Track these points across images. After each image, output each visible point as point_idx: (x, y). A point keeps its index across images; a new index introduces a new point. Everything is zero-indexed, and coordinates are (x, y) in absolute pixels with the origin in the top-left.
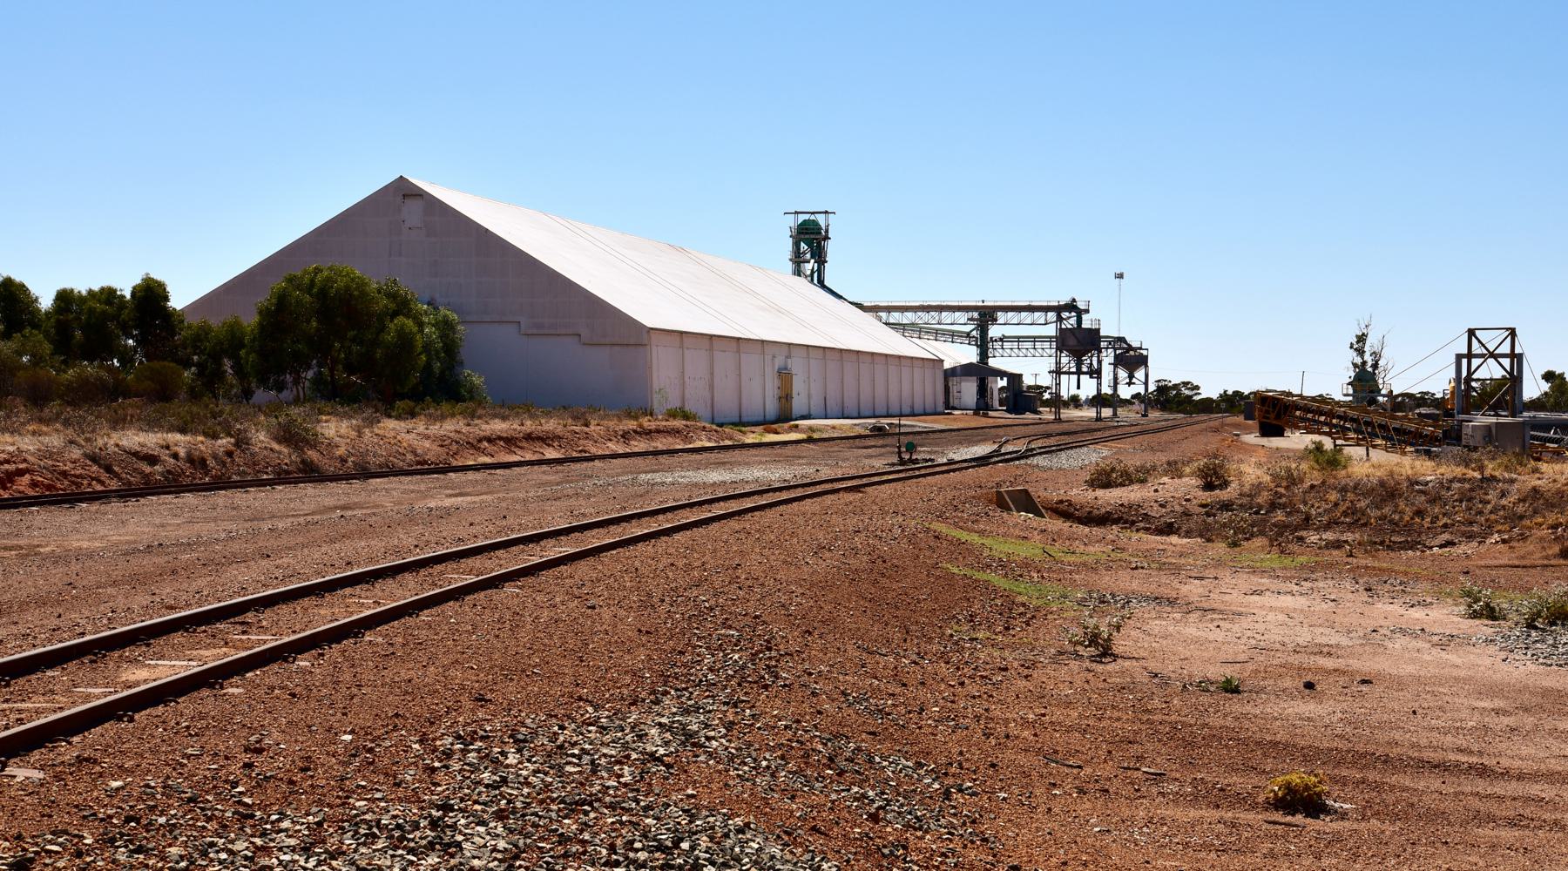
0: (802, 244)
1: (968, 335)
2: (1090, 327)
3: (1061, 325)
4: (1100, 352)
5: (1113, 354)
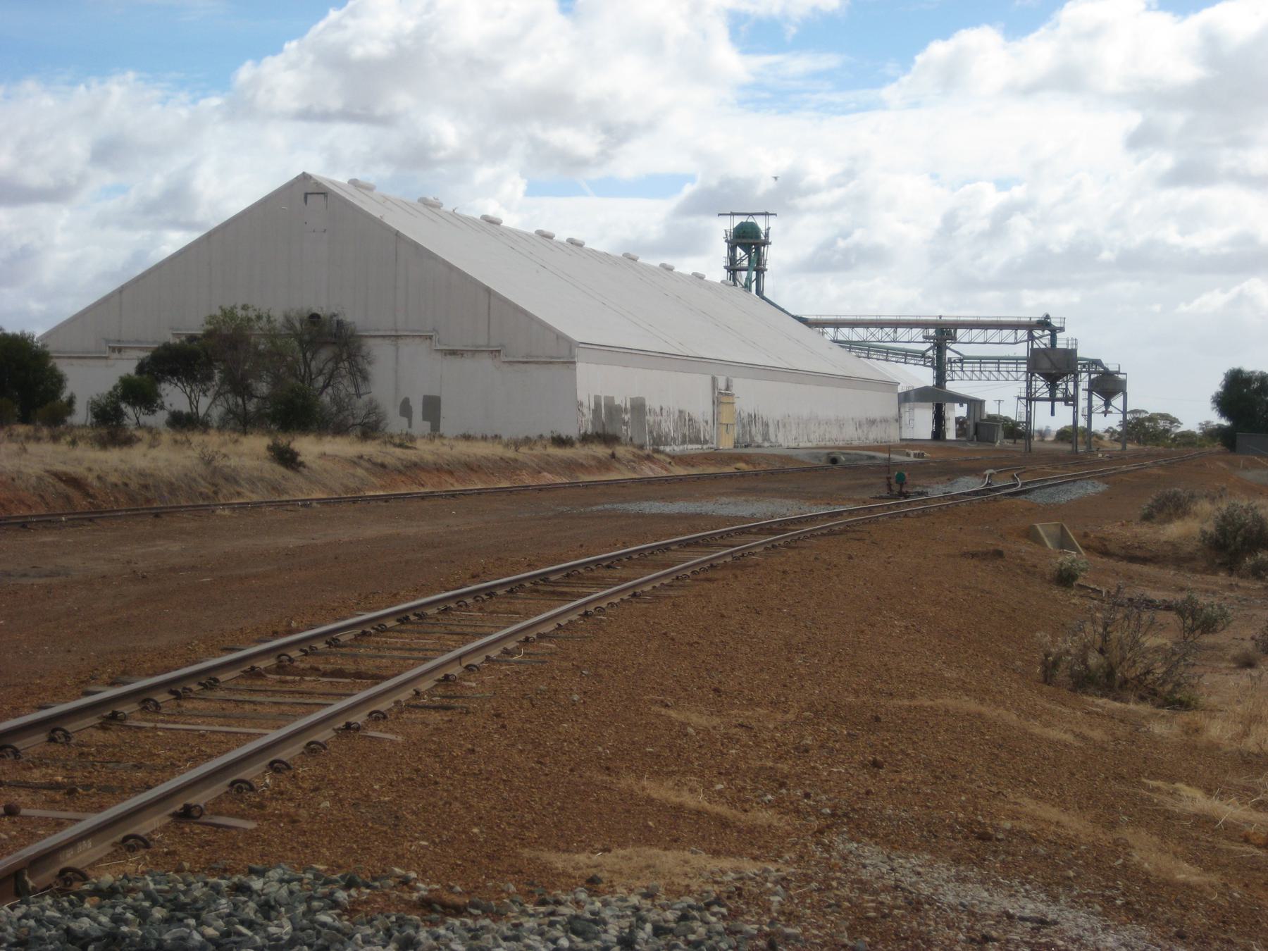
0: (739, 250)
1: (923, 355)
2: (1065, 347)
3: (1032, 346)
4: (1076, 376)
5: (1087, 378)
